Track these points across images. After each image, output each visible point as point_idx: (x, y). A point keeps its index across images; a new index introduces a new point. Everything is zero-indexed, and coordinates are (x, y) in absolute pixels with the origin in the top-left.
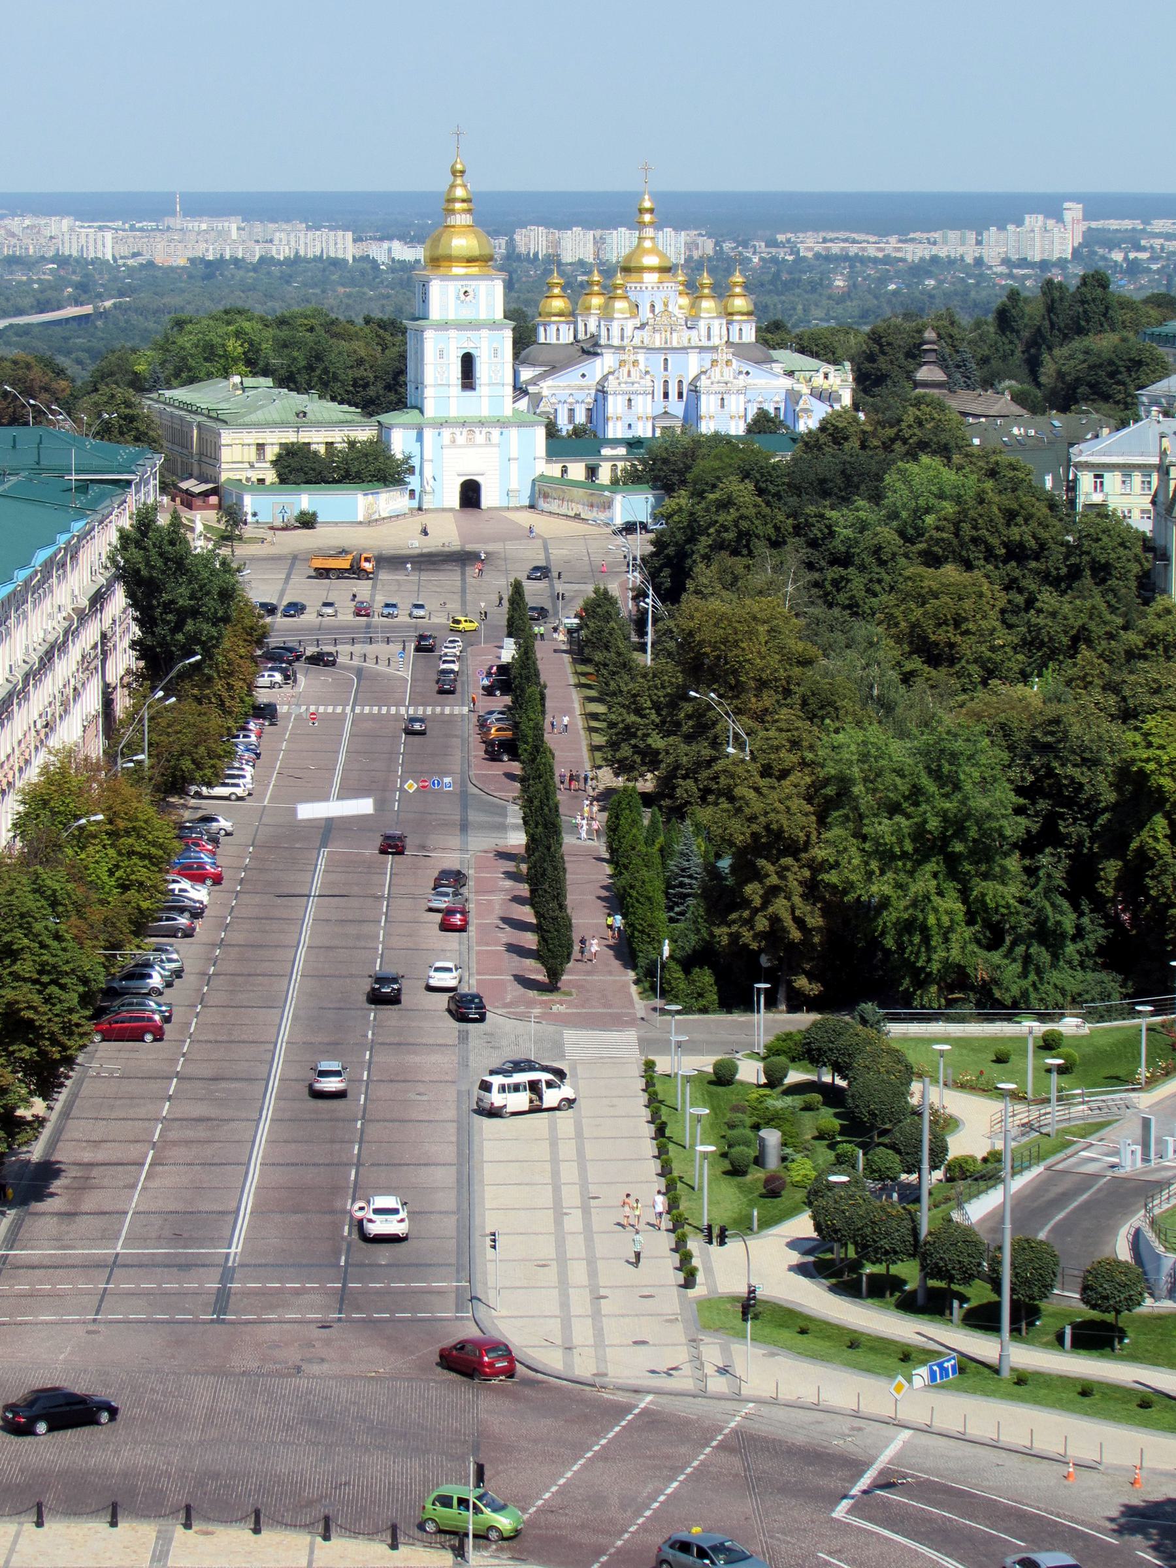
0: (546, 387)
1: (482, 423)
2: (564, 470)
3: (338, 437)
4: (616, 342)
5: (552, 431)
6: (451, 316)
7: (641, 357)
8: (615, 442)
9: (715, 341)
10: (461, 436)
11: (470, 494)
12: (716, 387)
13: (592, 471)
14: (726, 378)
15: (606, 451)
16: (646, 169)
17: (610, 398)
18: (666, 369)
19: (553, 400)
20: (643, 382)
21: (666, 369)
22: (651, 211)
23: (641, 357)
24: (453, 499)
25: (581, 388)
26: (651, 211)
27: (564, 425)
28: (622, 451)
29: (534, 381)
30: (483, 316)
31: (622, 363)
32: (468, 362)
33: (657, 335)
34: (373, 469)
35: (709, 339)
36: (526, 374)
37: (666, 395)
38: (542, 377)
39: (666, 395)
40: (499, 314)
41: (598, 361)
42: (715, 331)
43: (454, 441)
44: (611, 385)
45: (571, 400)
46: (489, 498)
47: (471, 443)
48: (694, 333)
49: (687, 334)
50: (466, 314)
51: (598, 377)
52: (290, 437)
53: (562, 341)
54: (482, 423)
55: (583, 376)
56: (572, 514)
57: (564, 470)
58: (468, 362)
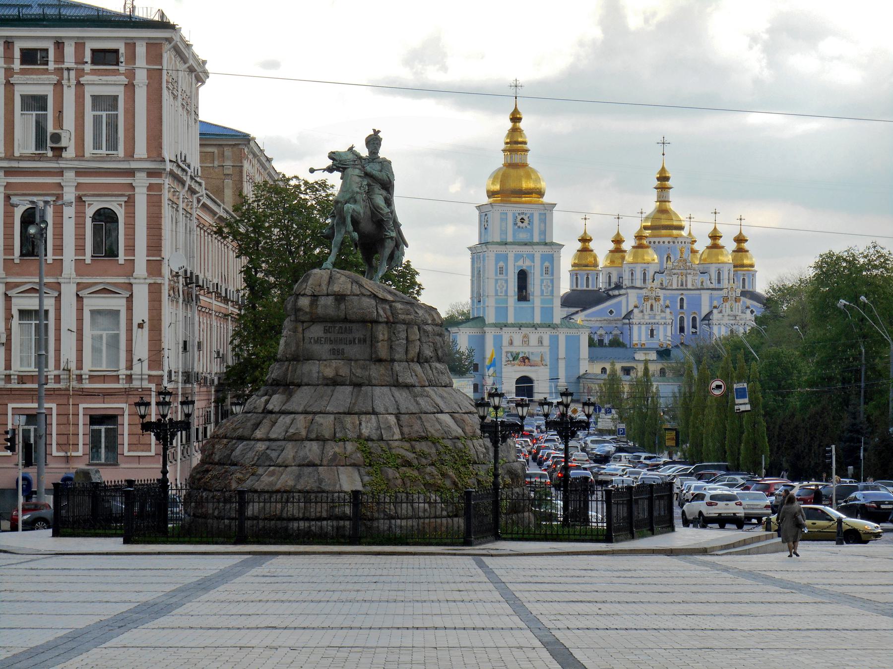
1: (535, 326)
4: (639, 283)
6: (510, 239)
7: (661, 293)
12: (726, 320)
14: (735, 312)
15: (640, 356)
17: (635, 328)
18: (682, 307)
20: (663, 315)
21: (682, 307)
25: (610, 321)
28: (653, 356)
31: (647, 298)
32: (523, 277)
33: (675, 278)
35: (719, 282)
38: (573, 314)
41: (623, 298)
42: (725, 276)
44: (637, 317)
48: (706, 277)
49: (699, 278)
50: (523, 236)
51: (624, 313)
53: (590, 288)
54: (535, 326)
55: (611, 312)
58: (523, 277)
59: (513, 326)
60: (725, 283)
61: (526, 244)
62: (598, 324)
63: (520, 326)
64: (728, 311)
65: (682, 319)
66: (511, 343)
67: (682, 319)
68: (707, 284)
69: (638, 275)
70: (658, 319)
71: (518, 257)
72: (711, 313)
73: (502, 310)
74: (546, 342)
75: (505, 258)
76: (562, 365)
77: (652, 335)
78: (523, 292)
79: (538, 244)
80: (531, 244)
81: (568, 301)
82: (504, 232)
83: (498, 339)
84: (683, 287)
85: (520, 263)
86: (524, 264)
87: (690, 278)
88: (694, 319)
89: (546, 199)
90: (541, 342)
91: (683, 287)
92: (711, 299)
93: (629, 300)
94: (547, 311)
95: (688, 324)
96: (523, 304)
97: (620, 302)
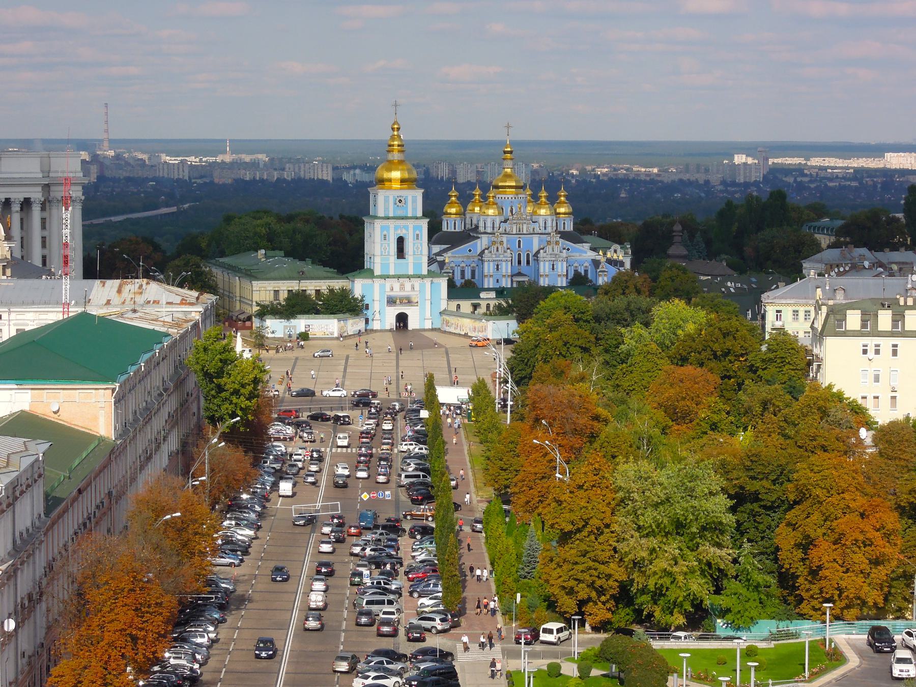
0: (447, 257)
1: (409, 277)
2: (458, 306)
3: (324, 286)
4: (489, 230)
5: (451, 284)
6: (391, 215)
7: (505, 239)
8: (489, 290)
9: (549, 230)
13: (475, 307)
14: (556, 252)
15: (482, 295)
16: (508, 127)
17: (486, 264)
18: (519, 246)
19: (453, 265)
21: (519, 246)
22: (511, 152)
23: (504, 240)
25: (468, 257)
27: (458, 281)
28: (493, 295)
29: (439, 254)
30: (410, 215)
31: (494, 243)
32: (401, 241)
34: (344, 305)
36: (436, 249)
37: (519, 262)
38: (445, 251)
39: (519, 262)
40: (420, 213)
41: (478, 241)
42: (549, 224)
50: (400, 213)
52: (294, 286)
54: (409, 277)
55: (470, 251)
56: (463, 333)
57: (458, 306)
58: (401, 241)
59: (393, 277)
60: (549, 230)
61: (403, 218)
62: (460, 260)
63: (398, 277)
64: (551, 251)
65: (519, 255)
66: (392, 289)
67: (519, 255)
68: (537, 230)
69: (489, 224)
71: (396, 228)
72: (538, 252)
73: (385, 266)
74: (417, 288)
75: (387, 228)
77: (498, 269)
78: (401, 252)
79: (411, 218)
80: (407, 218)
82: (386, 209)
83: (382, 287)
84: (520, 233)
85: (399, 232)
87: (525, 226)
88: (528, 255)
90: (413, 288)
91: (520, 233)
92: (540, 241)
93: (482, 242)
94: (417, 265)
95: (524, 259)
97: (476, 244)
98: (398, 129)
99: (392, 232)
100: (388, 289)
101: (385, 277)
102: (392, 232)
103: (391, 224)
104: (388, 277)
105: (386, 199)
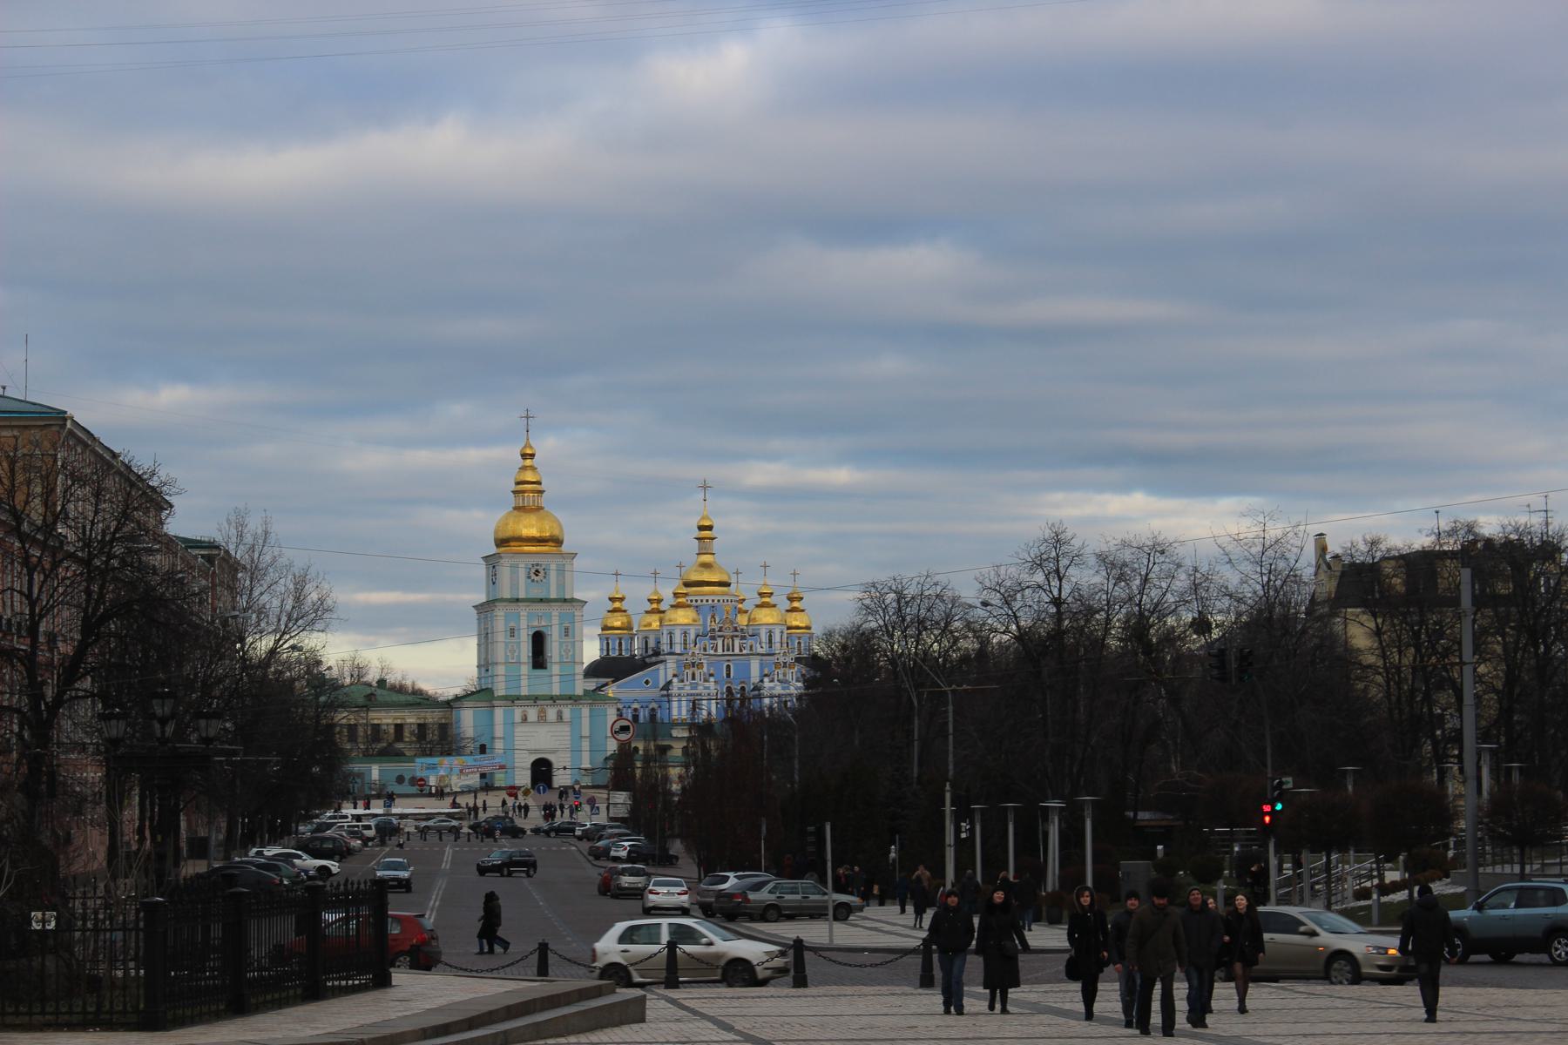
4: (678, 649)
6: (522, 596)
10: (533, 714)
11: (542, 771)
18: (728, 675)
21: (728, 675)
24: (523, 778)
26: (710, 528)
30: (553, 596)
32: (538, 640)
41: (661, 666)
43: (525, 720)
45: (636, 706)
46: (561, 779)
47: (542, 719)
50: (536, 593)
51: (662, 684)
54: (552, 698)
58: (538, 640)
59: (527, 698)
60: (777, 647)
69: (678, 638)
70: (700, 689)
71: (529, 617)
76: (586, 744)
81: (594, 671)
82: (514, 585)
86: (537, 624)
89: (565, 548)
93: (666, 670)
96: (539, 672)
98: (532, 456)
99: (524, 623)
100: (518, 718)
101: (513, 700)
102: (524, 623)
103: (524, 611)
104: (518, 698)
105: (514, 567)
